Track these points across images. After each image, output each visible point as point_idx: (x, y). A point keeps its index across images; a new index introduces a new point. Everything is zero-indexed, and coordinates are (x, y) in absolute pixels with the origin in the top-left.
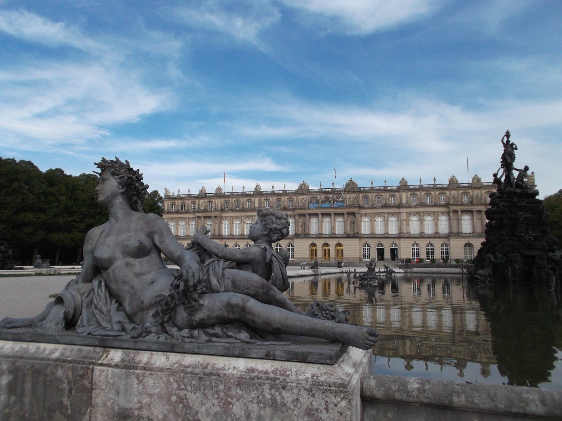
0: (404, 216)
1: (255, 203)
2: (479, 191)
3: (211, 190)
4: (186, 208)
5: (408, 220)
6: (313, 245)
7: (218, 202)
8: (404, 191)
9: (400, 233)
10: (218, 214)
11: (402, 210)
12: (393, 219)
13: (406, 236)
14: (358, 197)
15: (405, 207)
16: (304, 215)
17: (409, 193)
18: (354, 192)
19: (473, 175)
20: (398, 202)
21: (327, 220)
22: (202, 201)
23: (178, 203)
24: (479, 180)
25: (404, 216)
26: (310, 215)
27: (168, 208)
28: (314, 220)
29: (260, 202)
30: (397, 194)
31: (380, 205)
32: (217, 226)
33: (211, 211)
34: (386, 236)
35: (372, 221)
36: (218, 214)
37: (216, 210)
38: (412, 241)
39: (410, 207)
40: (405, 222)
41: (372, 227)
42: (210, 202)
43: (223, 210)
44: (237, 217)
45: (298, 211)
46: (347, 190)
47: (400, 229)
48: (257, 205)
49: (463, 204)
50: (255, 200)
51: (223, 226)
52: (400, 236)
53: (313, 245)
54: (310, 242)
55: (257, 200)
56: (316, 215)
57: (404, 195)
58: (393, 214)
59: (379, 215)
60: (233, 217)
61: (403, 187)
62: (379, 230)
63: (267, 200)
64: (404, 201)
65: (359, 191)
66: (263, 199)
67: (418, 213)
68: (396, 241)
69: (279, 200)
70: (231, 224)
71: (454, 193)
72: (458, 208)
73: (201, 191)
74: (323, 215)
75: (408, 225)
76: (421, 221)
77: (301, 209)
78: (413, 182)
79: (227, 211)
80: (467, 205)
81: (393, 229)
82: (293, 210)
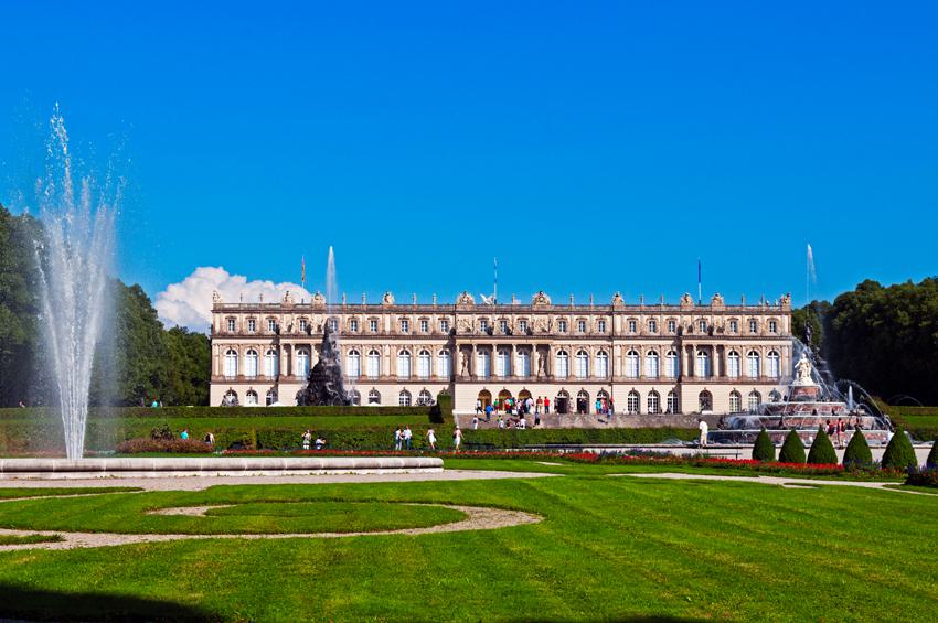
1: (383, 325)
2: (719, 317)
4: (258, 328)
6: (485, 393)
8: (619, 313)
11: (615, 342)
13: (621, 380)
15: (621, 338)
17: (627, 317)
22: (287, 317)
27: (221, 327)
29: (392, 323)
31: (582, 333)
39: (628, 338)
40: (619, 360)
45: (459, 342)
46: (535, 309)
48: (388, 329)
50: (384, 319)
53: (485, 393)
54: (480, 387)
55: (387, 317)
57: (618, 318)
64: (618, 329)
81: (599, 369)
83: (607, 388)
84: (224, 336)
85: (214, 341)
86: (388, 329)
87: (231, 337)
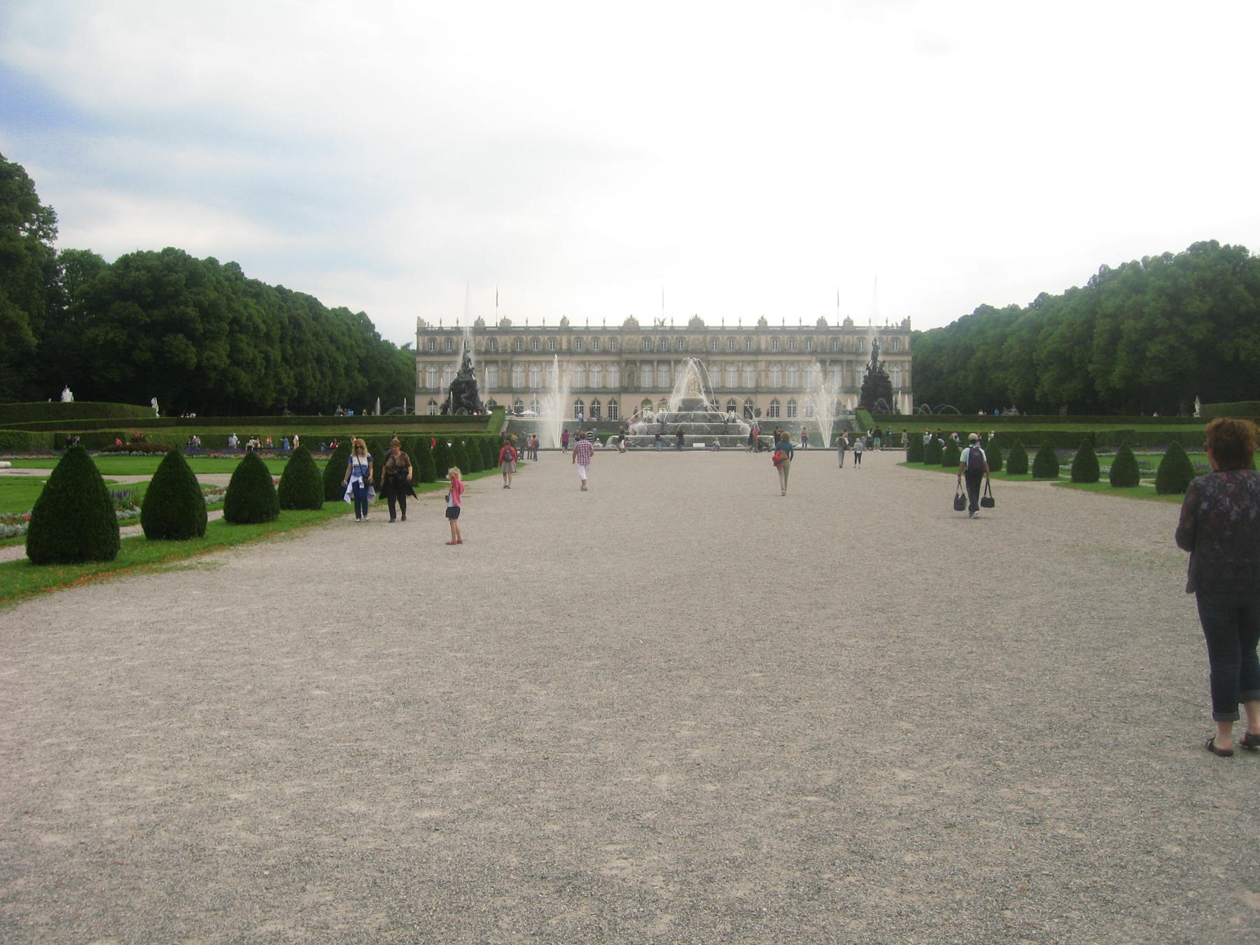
0: (762, 366)
3: (491, 322)
5: (767, 371)
7: (504, 341)
9: (757, 387)
10: (507, 357)
11: (760, 358)
12: (748, 369)
14: (705, 340)
15: (765, 354)
16: (634, 362)
18: (701, 333)
19: (845, 317)
20: (754, 346)
21: (664, 368)
23: (440, 339)
24: (851, 322)
25: (762, 366)
26: (643, 362)
28: (647, 368)
29: (569, 342)
30: (755, 337)
32: (505, 374)
33: (497, 353)
34: (740, 391)
35: (723, 371)
36: (507, 357)
37: (505, 352)
38: (771, 397)
41: (723, 378)
42: (493, 340)
43: (514, 352)
44: (535, 363)
45: (625, 357)
47: (757, 381)
48: (564, 347)
49: (831, 353)
51: (514, 375)
52: (757, 391)
54: (643, 397)
56: (651, 362)
58: (749, 363)
59: (732, 363)
60: (529, 362)
61: (762, 328)
62: (731, 381)
63: (579, 339)
64: (763, 347)
65: (705, 331)
66: (573, 338)
67: (780, 362)
68: (753, 398)
69: (596, 339)
70: (527, 372)
71: (823, 337)
72: (828, 357)
73: (477, 323)
74: (660, 362)
75: (767, 376)
76: (783, 372)
77: (631, 353)
78: (774, 322)
79: (521, 354)
80: (837, 353)
81: (750, 384)
82: (620, 353)
83: (753, 398)
84: (425, 353)
85: (418, 359)
86: (564, 347)
87: (432, 354)
